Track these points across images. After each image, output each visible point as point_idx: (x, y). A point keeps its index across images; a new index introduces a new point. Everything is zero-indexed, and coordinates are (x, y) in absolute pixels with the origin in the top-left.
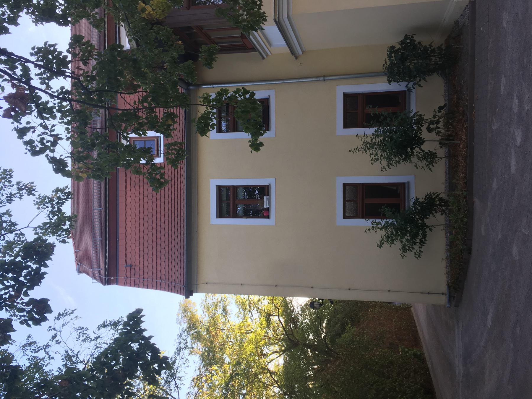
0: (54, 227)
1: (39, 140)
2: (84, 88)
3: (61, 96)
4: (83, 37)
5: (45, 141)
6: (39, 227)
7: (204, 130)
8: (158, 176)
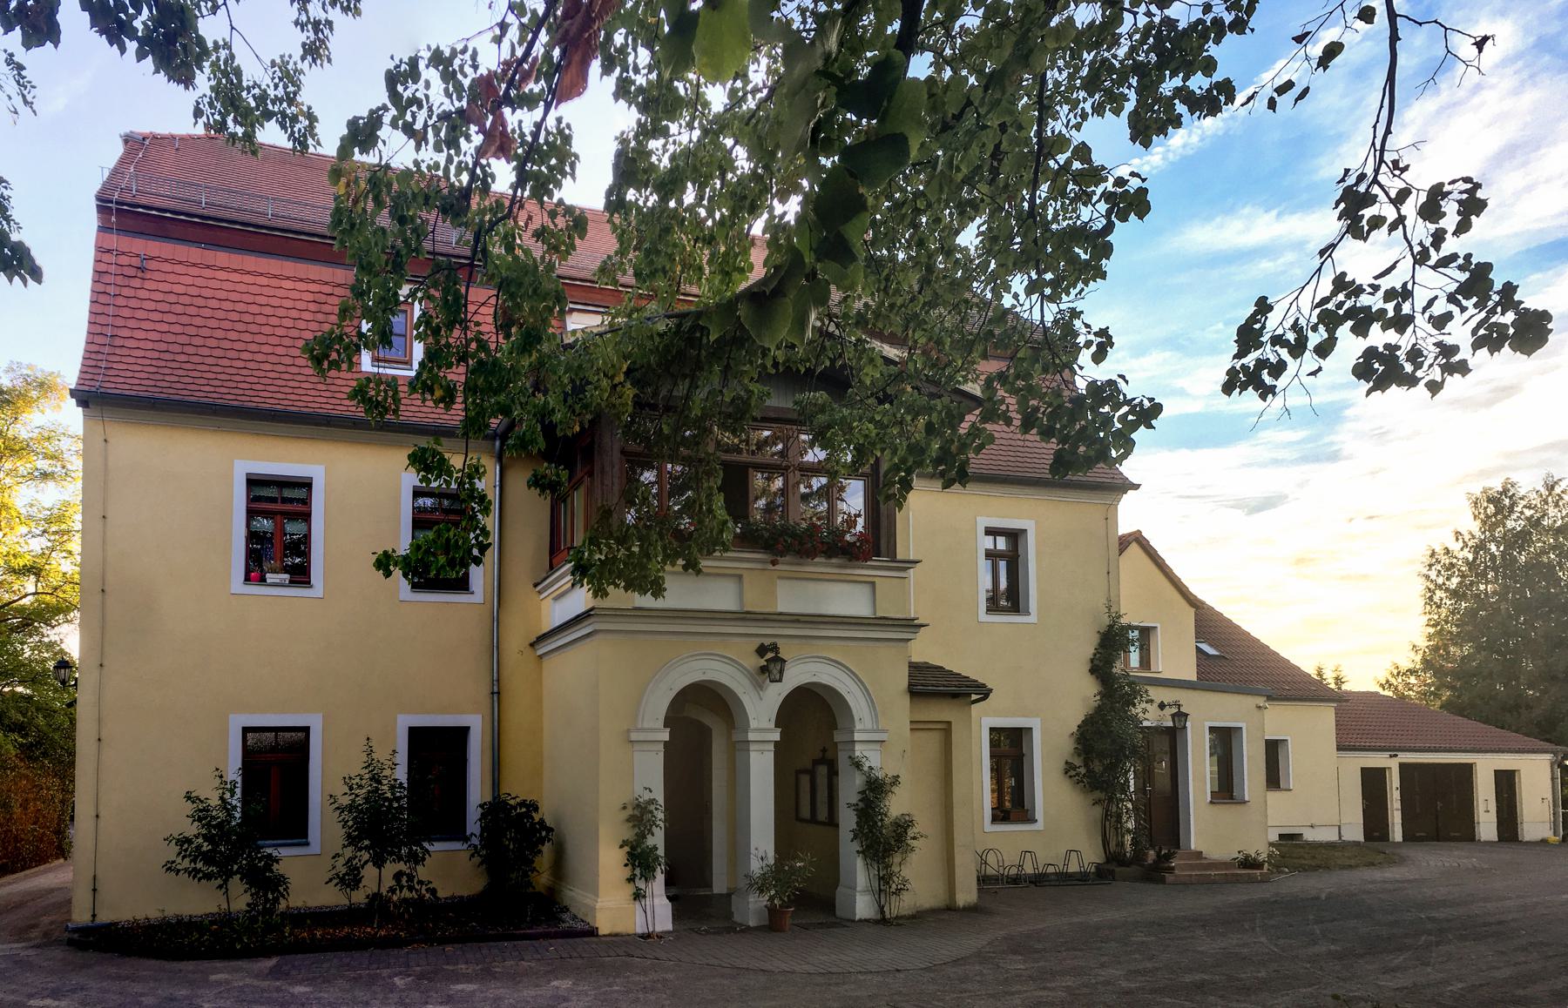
0: (229, 93)
1: (418, 95)
2: (493, 224)
3: (478, 171)
4: (582, 238)
5: (414, 108)
6: (232, 57)
7: (420, 461)
8: (334, 356)
